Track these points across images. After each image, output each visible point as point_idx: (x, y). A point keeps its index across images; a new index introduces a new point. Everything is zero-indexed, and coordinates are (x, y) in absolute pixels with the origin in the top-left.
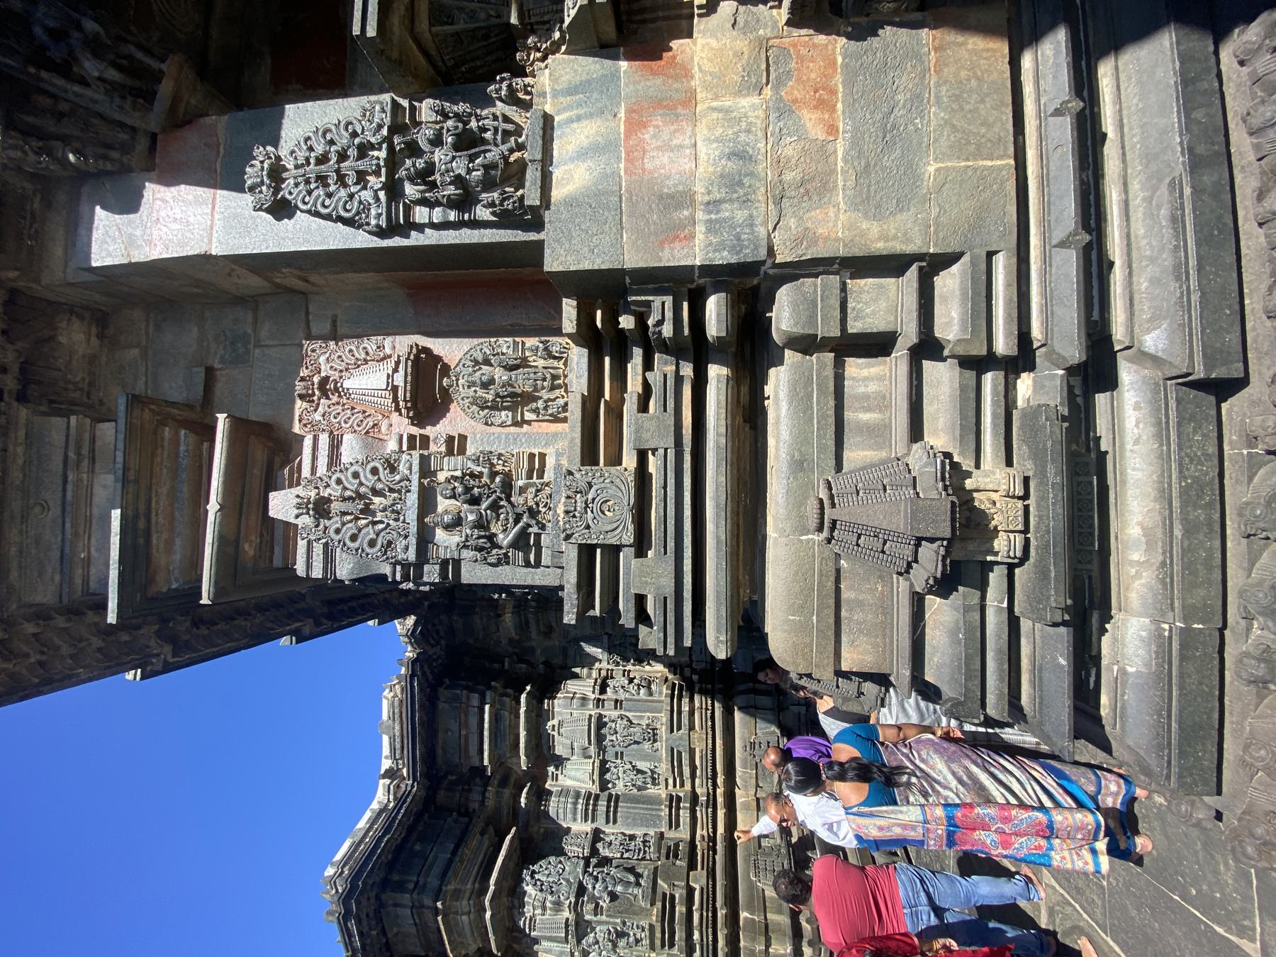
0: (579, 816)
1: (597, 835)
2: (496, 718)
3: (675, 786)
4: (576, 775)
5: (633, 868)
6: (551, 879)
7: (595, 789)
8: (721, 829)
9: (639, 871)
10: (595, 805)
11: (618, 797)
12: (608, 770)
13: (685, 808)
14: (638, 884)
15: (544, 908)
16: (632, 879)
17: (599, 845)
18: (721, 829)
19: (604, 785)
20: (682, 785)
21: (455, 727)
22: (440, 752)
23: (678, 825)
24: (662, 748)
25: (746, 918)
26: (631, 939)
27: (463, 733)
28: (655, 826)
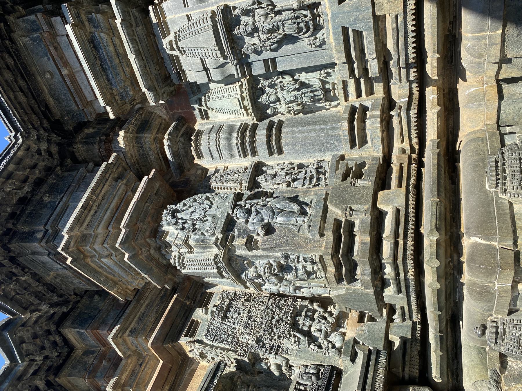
0: (236, 152)
1: (258, 169)
2: (92, 46)
3: (359, 95)
4: (225, 107)
5: (297, 197)
6: (194, 217)
7: (250, 120)
8: (432, 134)
9: (307, 200)
10: (253, 136)
11: (281, 123)
12: (263, 92)
13: (373, 117)
14: (303, 213)
15: (189, 247)
16: (295, 208)
17: (261, 179)
18: (432, 134)
19: (261, 112)
20: (371, 92)
21: (51, 66)
22: (51, 101)
23: (364, 142)
24: (330, 34)
25: (475, 247)
26: (301, 272)
27: (65, 72)
28: (333, 148)
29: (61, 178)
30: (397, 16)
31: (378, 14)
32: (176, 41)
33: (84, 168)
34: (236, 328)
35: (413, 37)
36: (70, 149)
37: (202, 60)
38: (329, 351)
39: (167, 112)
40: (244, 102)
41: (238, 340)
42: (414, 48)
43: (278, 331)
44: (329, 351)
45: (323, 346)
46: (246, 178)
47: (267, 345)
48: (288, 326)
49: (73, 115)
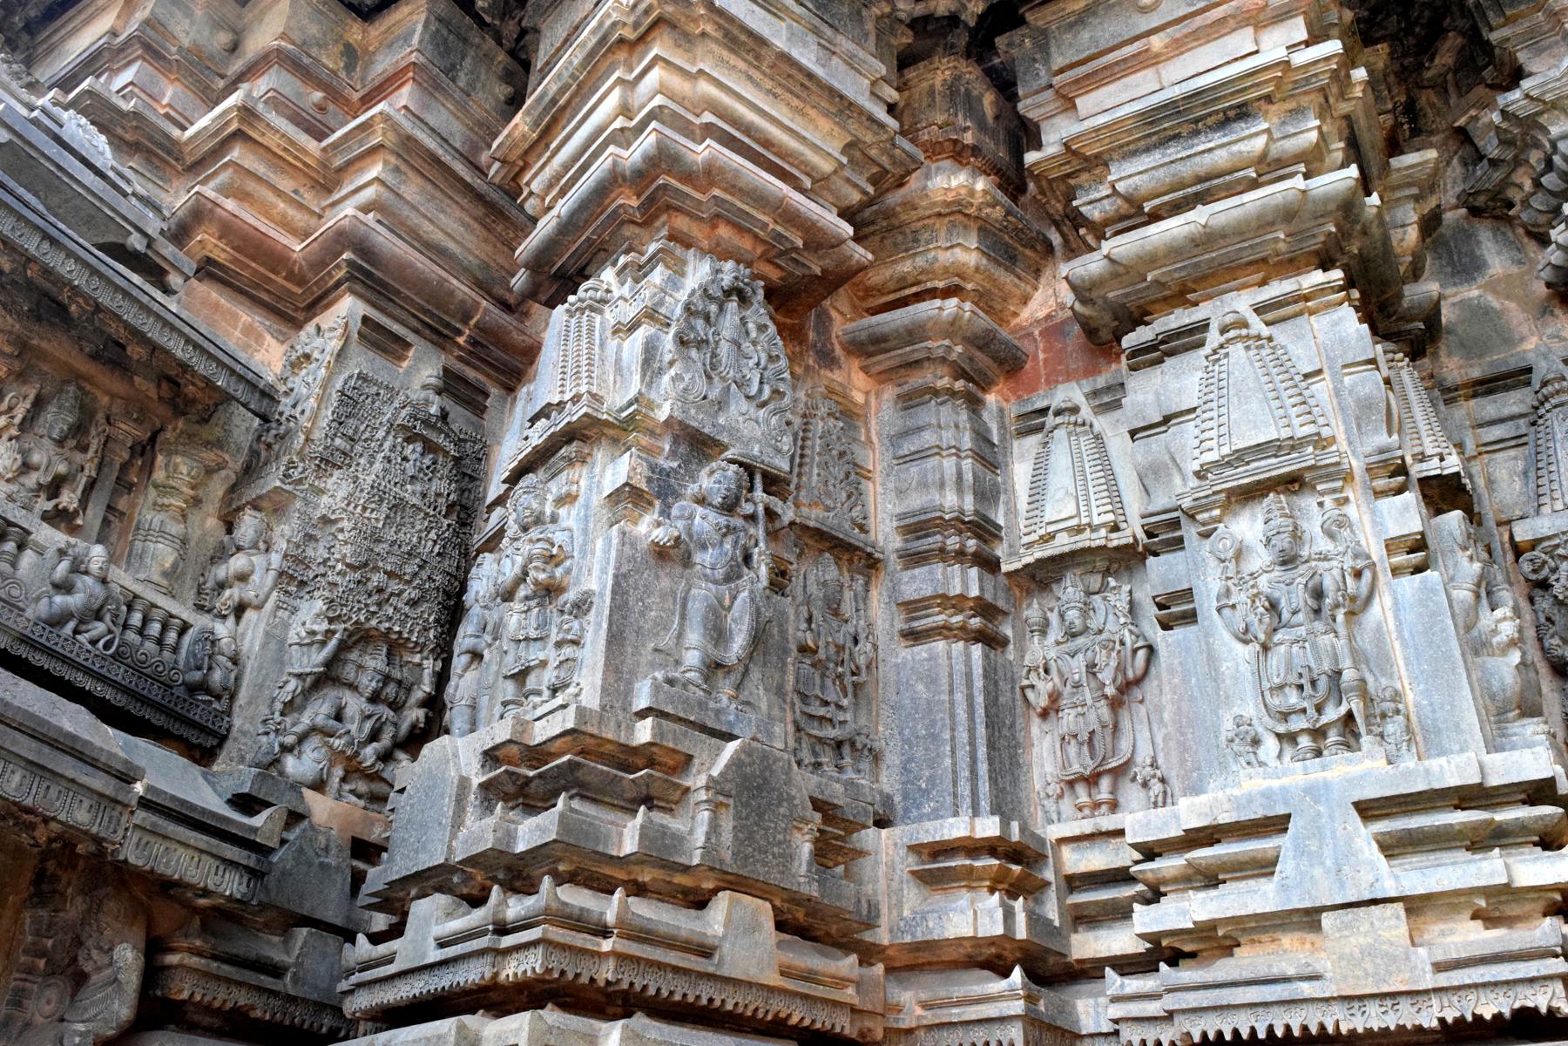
27: (1157, 42)
29: (859, 13)
30: (1314, 977)
31: (1327, 920)
32: (1248, 337)
33: (884, 72)
34: (372, 464)
35: (1253, 1031)
36: (940, 50)
37: (1195, 409)
38: (272, 735)
39: (1038, 322)
40: (1065, 534)
41: (334, 465)
42: (1220, 1034)
43: (352, 586)
44: (272, 735)
45: (288, 720)
46: (835, 520)
47: (310, 552)
48: (362, 618)
49: (1035, 60)
